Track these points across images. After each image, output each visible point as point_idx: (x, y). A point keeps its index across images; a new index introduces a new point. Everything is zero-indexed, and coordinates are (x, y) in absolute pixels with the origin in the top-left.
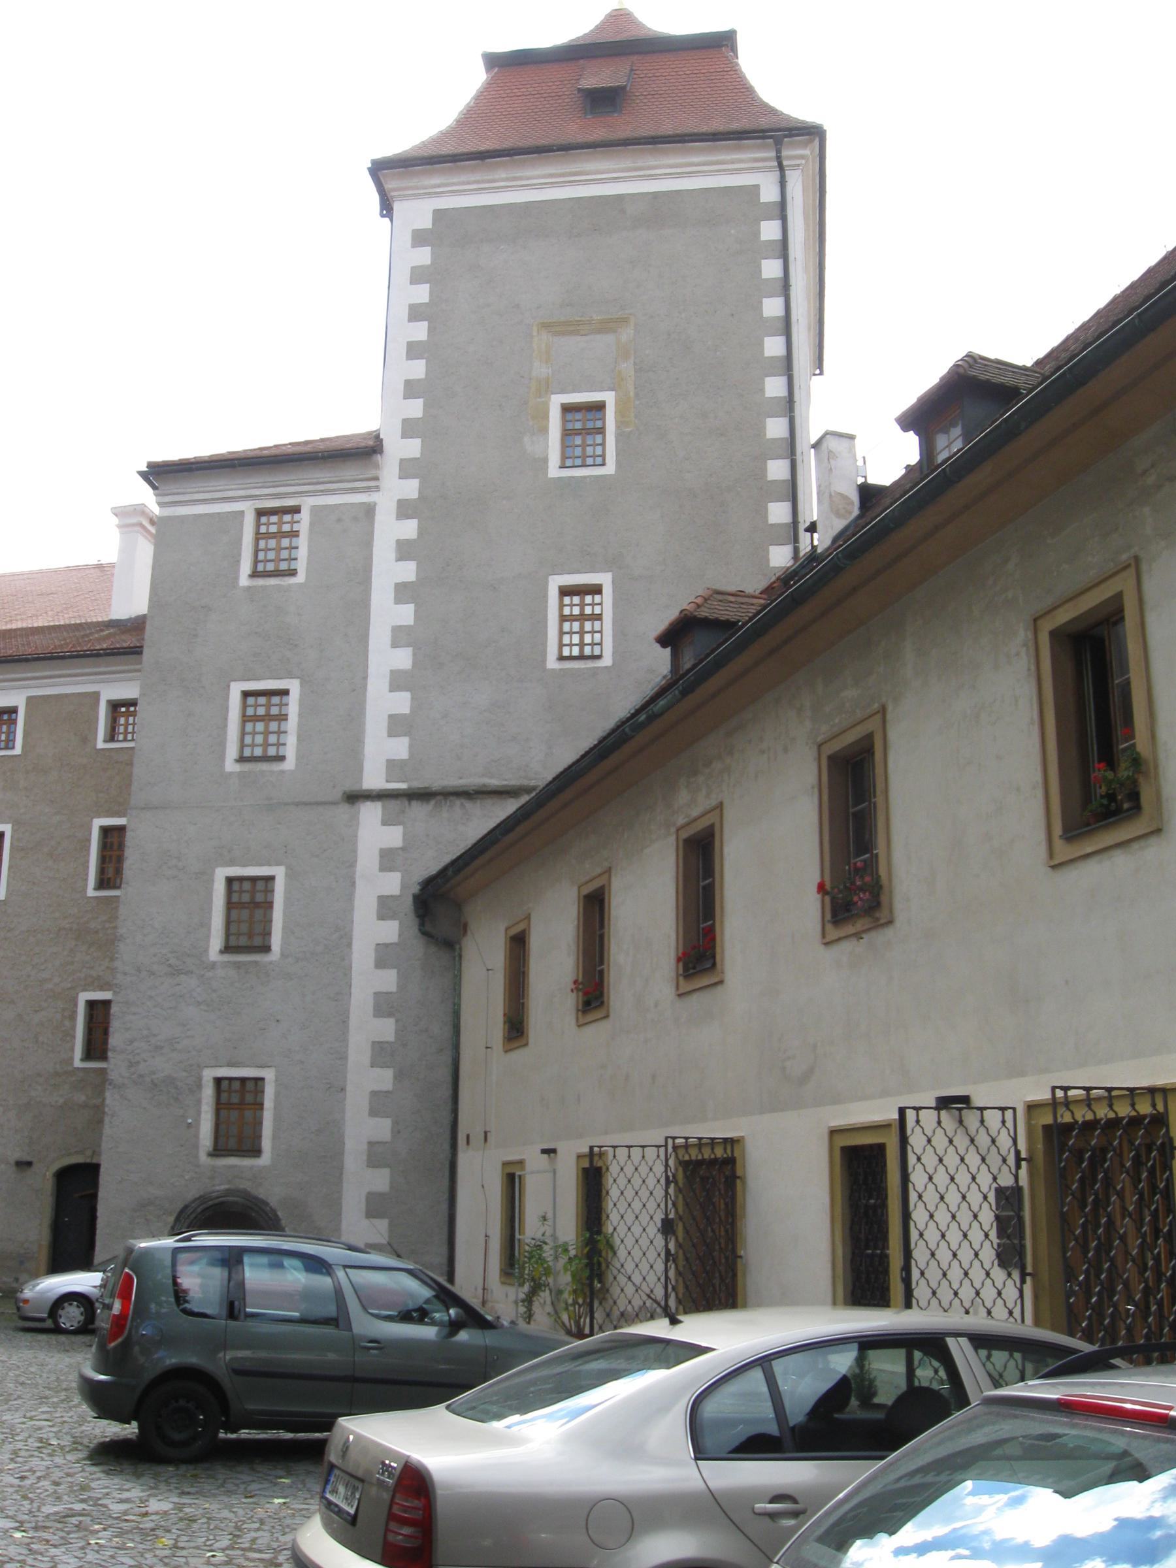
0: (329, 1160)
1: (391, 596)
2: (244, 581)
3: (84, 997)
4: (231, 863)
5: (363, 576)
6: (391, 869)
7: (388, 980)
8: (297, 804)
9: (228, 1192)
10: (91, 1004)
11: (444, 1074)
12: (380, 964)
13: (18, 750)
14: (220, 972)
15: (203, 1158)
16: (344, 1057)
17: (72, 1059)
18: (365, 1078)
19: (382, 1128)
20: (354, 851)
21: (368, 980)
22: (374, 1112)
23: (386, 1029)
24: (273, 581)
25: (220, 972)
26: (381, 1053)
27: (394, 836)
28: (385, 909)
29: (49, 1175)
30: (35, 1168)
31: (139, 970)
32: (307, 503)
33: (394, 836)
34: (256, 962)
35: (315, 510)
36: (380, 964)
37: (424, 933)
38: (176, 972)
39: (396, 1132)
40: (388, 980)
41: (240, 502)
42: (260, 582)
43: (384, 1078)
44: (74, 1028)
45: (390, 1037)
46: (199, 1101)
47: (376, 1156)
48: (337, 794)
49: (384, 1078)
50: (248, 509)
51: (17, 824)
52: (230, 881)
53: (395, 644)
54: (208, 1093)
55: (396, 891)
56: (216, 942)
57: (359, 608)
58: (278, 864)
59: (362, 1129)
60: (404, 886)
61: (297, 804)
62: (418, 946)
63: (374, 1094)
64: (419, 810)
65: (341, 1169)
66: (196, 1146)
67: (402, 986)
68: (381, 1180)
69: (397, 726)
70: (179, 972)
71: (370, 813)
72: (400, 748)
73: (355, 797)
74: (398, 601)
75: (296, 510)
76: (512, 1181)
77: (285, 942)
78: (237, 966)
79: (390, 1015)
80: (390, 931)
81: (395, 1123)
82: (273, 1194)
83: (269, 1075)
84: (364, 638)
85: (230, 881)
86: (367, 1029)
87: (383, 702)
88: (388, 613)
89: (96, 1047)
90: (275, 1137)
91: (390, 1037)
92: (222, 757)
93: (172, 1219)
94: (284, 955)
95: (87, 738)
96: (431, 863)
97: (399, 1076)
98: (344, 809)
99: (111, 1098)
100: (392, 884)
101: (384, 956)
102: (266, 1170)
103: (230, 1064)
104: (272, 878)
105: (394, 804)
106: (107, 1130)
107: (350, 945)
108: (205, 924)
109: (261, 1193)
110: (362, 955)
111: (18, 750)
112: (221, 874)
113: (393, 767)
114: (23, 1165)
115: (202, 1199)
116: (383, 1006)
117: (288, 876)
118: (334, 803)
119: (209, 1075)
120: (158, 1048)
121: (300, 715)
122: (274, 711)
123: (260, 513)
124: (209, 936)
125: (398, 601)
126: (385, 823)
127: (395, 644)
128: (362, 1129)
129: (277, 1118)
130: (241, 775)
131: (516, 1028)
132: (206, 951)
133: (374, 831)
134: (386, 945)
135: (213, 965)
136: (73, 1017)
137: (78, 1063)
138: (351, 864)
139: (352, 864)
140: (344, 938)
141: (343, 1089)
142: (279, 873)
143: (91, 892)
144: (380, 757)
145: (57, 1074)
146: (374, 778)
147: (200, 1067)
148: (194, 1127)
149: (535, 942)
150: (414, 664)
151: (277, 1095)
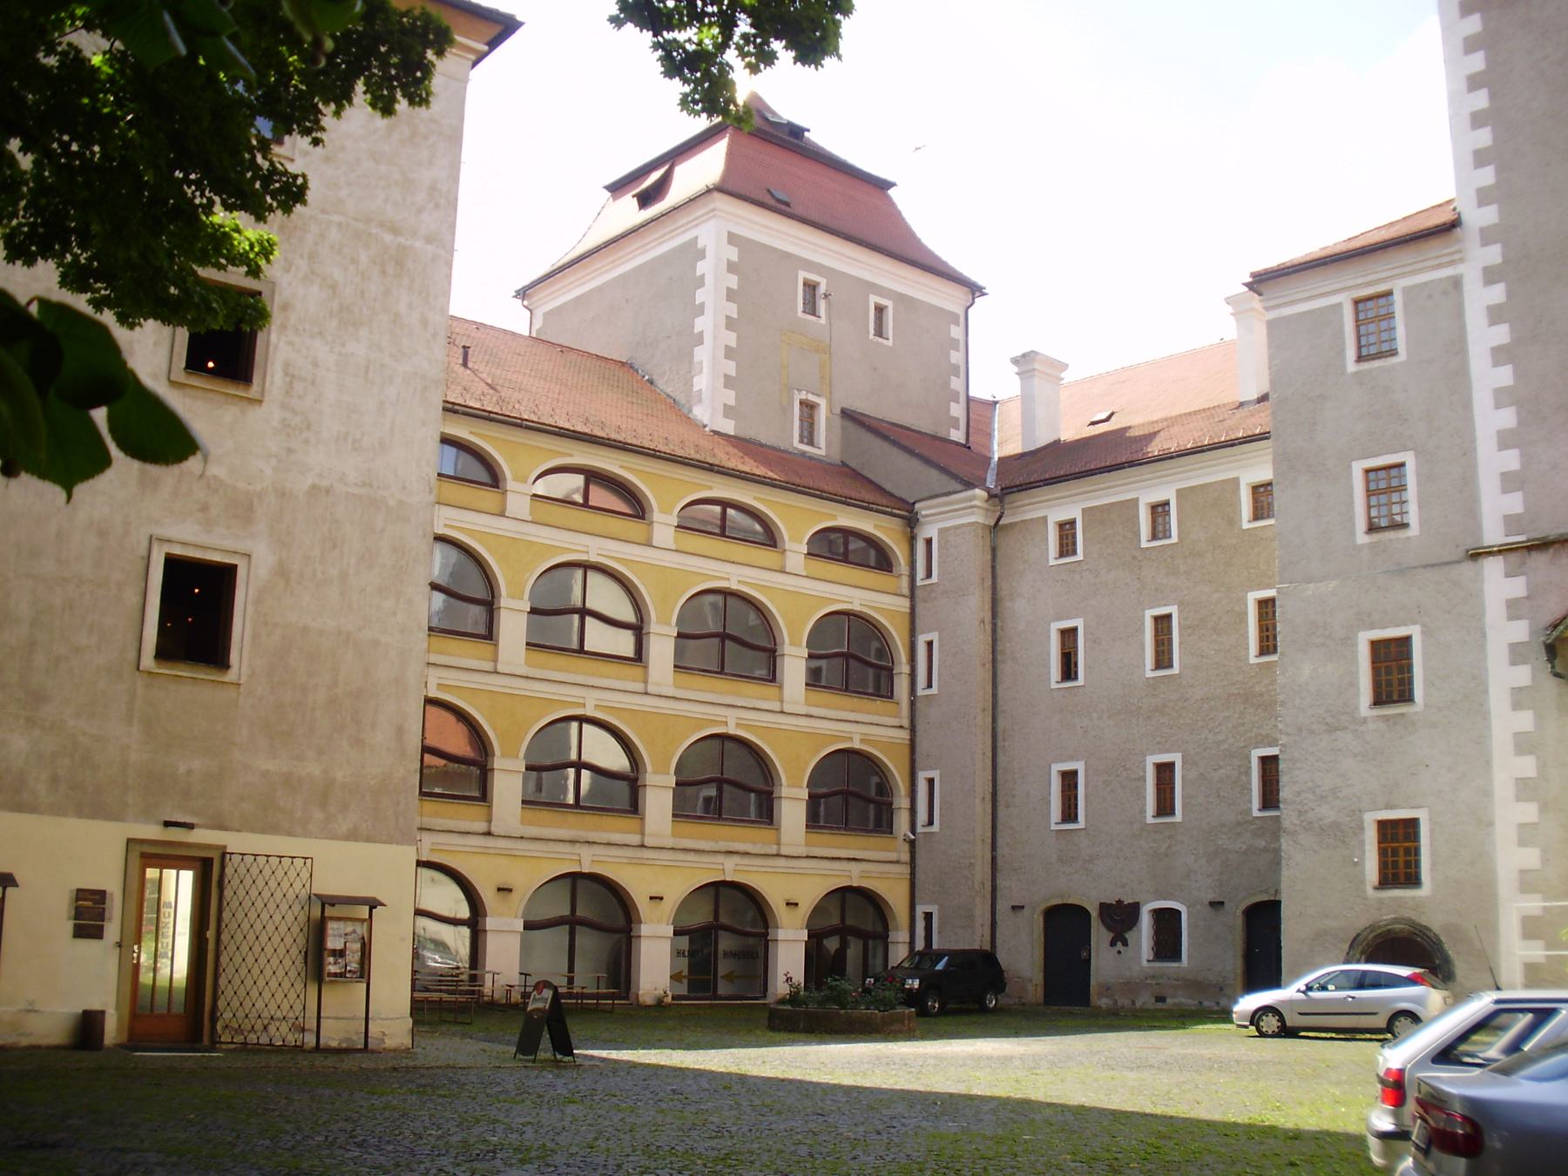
1: (1489, 360)
2: (1351, 366)
3: (1257, 753)
4: (1372, 627)
5: (1458, 346)
6: (1518, 618)
8: (1425, 567)
9: (1395, 921)
13: (1174, 539)
15: (1370, 892)
24: (1376, 364)
25: (1371, 726)
27: (1517, 587)
29: (1239, 912)
31: (1300, 730)
32: (1398, 286)
33: (1517, 587)
34: (1403, 714)
35: (1407, 291)
36: (1517, 706)
39: (1545, 860)
40: (1525, 721)
41: (1337, 295)
42: (1366, 366)
46: (1362, 843)
48: (1460, 553)
50: (1345, 300)
51: (1181, 605)
53: (1498, 406)
54: (1371, 836)
57: (1459, 376)
58: (1414, 623)
60: (1532, 633)
61: (1425, 567)
63: (1522, 826)
64: (1540, 560)
66: (1363, 882)
69: (1510, 482)
70: (1336, 729)
71: (1493, 568)
72: (1515, 503)
73: (1476, 555)
74: (1496, 364)
75: (1389, 294)
77: (1427, 695)
78: (1386, 718)
79: (1530, 753)
84: (1467, 406)
87: (1494, 462)
88: (1488, 377)
89: (1270, 798)
92: (1353, 533)
93: (1346, 946)
95: (1232, 520)
97: (1544, 808)
98: (1468, 568)
99: (1285, 844)
100: (1520, 631)
101: (1520, 699)
102: (1426, 902)
103: (1388, 807)
104: (1406, 640)
105: (1514, 558)
107: (1486, 691)
108: (1353, 684)
109: (1424, 921)
111: (1174, 539)
112: (1364, 638)
113: (1511, 522)
114: (1216, 905)
115: (1372, 928)
117: (1426, 633)
118: (1458, 562)
119: (1371, 819)
120: (1322, 797)
121: (1419, 484)
122: (1395, 483)
123: (1357, 302)
124: (1358, 695)
125: (1496, 364)
126: (1508, 575)
127: (1498, 406)
129: (1434, 853)
130: (1371, 546)
132: (1357, 708)
133: (1498, 584)
134: (1521, 689)
135: (1365, 721)
136: (1248, 772)
138: (1479, 616)
141: (1491, 824)
142: (1414, 631)
143: (1253, 660)
144: (1497, 513)
145: (1239, 824)
146: (1494, 535)
148: (1359, 865)
150: (1520, 422)
151: (1432, 831)
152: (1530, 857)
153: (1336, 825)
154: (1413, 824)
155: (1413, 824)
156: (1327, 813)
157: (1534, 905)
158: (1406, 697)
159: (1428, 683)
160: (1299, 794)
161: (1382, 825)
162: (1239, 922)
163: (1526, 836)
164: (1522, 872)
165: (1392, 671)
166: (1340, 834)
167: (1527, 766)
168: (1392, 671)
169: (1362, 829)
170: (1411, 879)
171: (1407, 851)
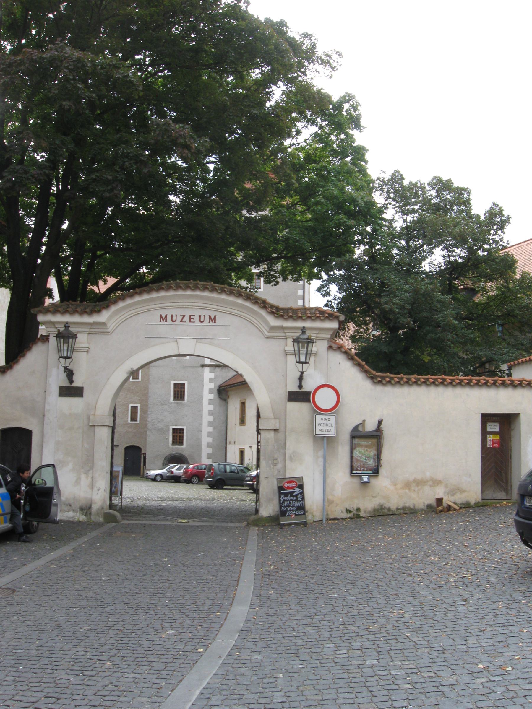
3: (130, 406)
7: (211, 407)
9: (176, 453)
10: (132, 407)
11: (224, 428)
12: (209, 404)
14: (173, 405)
15: (170, 446)
16: (201, 424)
17: (128, 421)
18: (206, 429)
19: (210, 440)
20: (203, 378)
21: (207, 407)
22: (208, 436)
23: (211, 418)
25: (173, 405)
26: (210, 424)
28: (211, 392)
30: (119, 446)
31: (154, 404)
36: (209, 404)
37: (220, 398)
38: (163, 404)
39: (213, 440)
40: (211, 407)
43: (211, 429)
44: (128, 413)
45: (212, 420)
46: (169, 434)
47: (209, 446)
48: (199, 365)
49: (211, 429)
52: (175, 384)
54: (171, 432)
55: (213, 388)
56: (172, 398)
59: (206, 440)
62: (218, 400)
63: (209, 432)
64: (218, 369)
65: (201, 448)
66: (169, 443)
67: (214, 409)
68: (210, 451)
70: (164, 405)
71: (207, 370)
73: (203, 366)
76: (242, 452)
78: (177, 403)
81: (213, 438)
82: (186, 454)
83: (185, 428)
85: (175, 384)
86: (207, 418)
90: (187, 441)
91: (212, 420)
93: (163, 459)
94: (188, 401)
96: (220, 382)
97: (214, 429)
98: (200, 369)
99: (148, 433)
102: (184, 449)
103: (176, 425)
104: (184, 384)
105: (212, 368)
106: (148, 440)
109: (184, 454)
110: (205, 402)
112: (173, 382)
115: (170, 455)
116: (210, 413)
117: (189, 383)
119: (171, 428)
128: (206, 440)
129: (187, 437)
131: (243, 421)
135: (171, 403)
136: (128, 410)
137: (129, 422)
139: (203, 381)
140: (201, 398)
142: (186, 383)
145: (124, 424)
147: (169, 426)
148: (168, 439)
149: (247, 405)
151: (187, 433)
152: (210, 440)
153: (162, 429)
154: (183, 429)
155: (183, 429)
156: (160, 425)
158: (182, 398)
159: (188, 396)
160: (153, 420)
161: (174, 429)
162: (123, 451)
164: (208, 443)
165: (179, 392)
166: (162, 431)
167: (211, 418)
168: (179, 392)
169: (169, 430)
170: (181, 443)
171: (180, 436)
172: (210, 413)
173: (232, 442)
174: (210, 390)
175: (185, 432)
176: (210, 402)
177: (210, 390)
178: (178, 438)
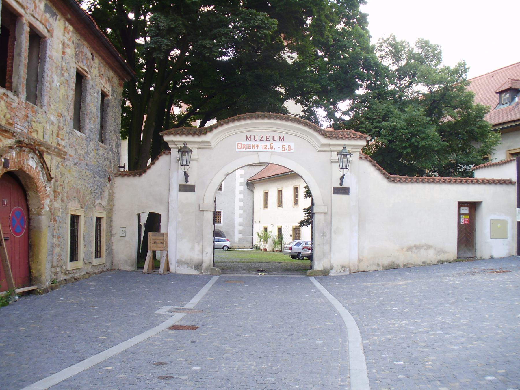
0: (233, 225)
7: (242, 196)
12: (240, 193)
16: (234, 208)
18: (238, 212)
19: (241, 220)
21: (239, 196)
22: (240, 217)
23: (241, 204)
28: (241, 184)
36: (240, 193)
39: (243, 220)
40: (242, 196)
49: (241, 212)
80: (242, 188)
82: (223, 230)
83: (222, 211)
86: (238, 204)
96: (248, 177)
97: (244, 211)
102: (221, 227)
110: (237, 192)
116: (241, 200)
128: (238, 220)
129: (224, 218)
140: (234, 189)
149: (269, 194)
154: (221, 212)
155: (221, 212)
157: (241, 228)
163: (240, 216)
167: (241, 204)
170: (220, 222)
172: (241, 200)
173: (258, 221)
174: (241, 183)
175: (222, 214)
176: (241, 192)
177: (241, 183)
178: (217, 219)
